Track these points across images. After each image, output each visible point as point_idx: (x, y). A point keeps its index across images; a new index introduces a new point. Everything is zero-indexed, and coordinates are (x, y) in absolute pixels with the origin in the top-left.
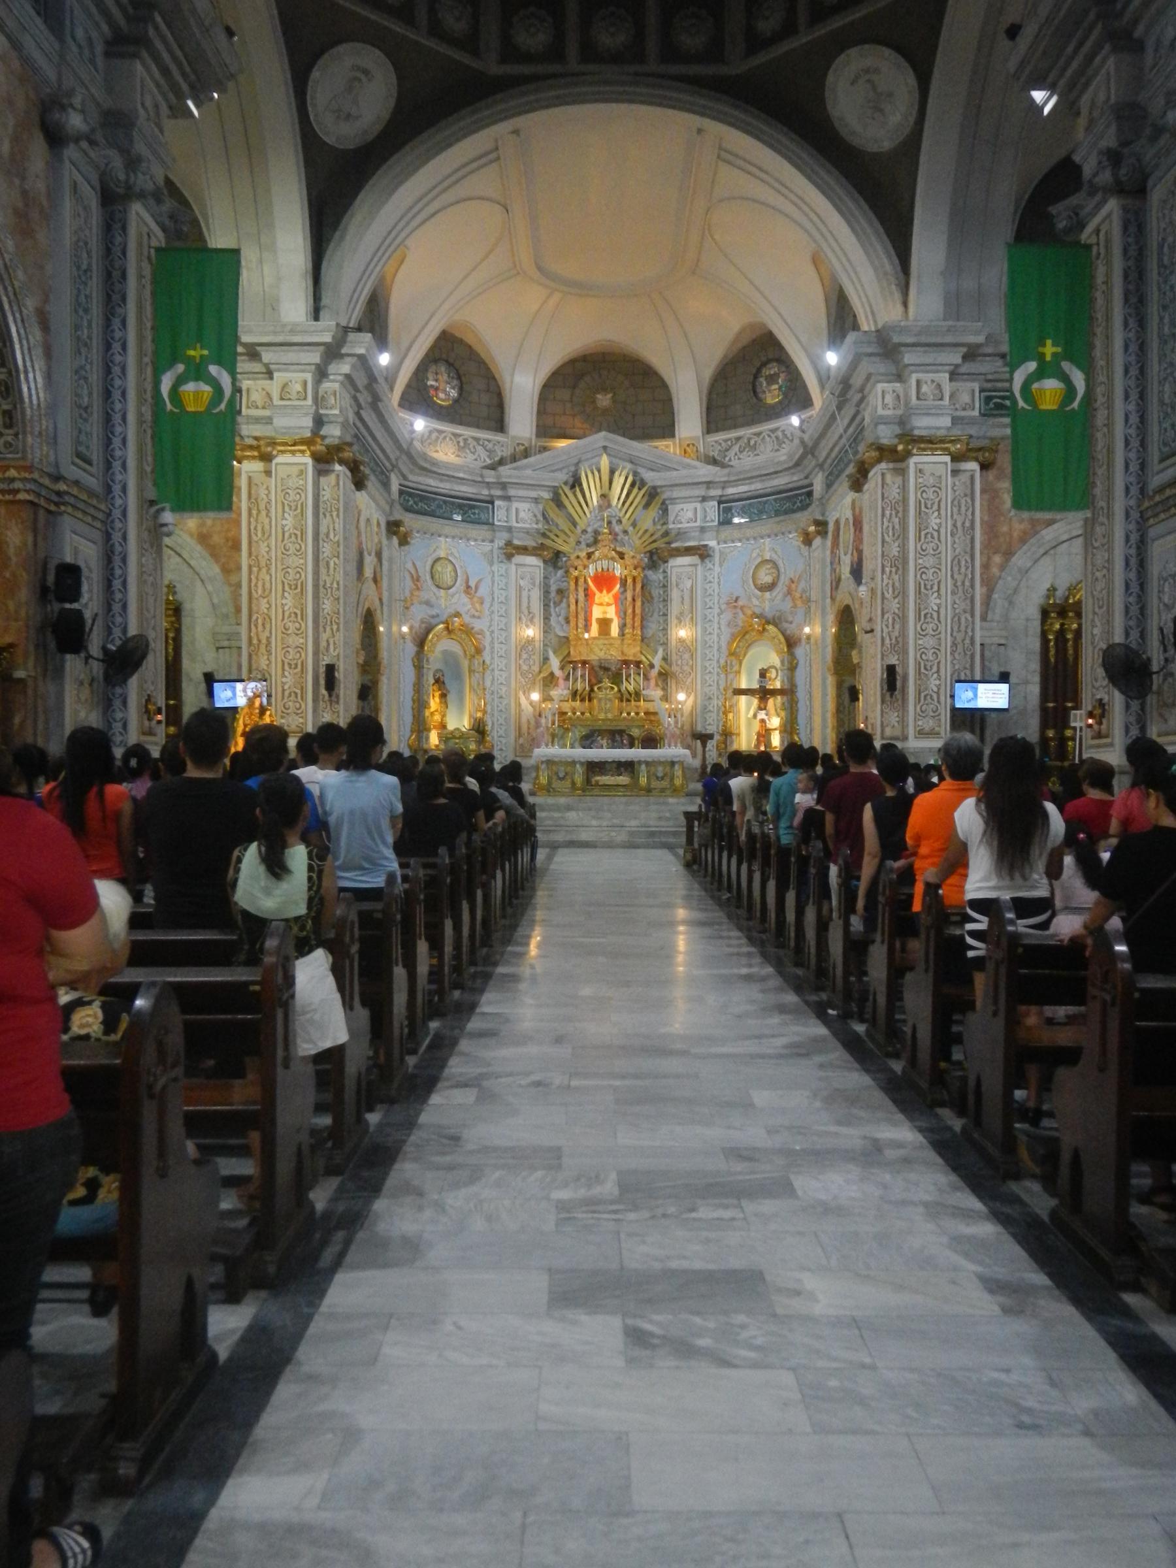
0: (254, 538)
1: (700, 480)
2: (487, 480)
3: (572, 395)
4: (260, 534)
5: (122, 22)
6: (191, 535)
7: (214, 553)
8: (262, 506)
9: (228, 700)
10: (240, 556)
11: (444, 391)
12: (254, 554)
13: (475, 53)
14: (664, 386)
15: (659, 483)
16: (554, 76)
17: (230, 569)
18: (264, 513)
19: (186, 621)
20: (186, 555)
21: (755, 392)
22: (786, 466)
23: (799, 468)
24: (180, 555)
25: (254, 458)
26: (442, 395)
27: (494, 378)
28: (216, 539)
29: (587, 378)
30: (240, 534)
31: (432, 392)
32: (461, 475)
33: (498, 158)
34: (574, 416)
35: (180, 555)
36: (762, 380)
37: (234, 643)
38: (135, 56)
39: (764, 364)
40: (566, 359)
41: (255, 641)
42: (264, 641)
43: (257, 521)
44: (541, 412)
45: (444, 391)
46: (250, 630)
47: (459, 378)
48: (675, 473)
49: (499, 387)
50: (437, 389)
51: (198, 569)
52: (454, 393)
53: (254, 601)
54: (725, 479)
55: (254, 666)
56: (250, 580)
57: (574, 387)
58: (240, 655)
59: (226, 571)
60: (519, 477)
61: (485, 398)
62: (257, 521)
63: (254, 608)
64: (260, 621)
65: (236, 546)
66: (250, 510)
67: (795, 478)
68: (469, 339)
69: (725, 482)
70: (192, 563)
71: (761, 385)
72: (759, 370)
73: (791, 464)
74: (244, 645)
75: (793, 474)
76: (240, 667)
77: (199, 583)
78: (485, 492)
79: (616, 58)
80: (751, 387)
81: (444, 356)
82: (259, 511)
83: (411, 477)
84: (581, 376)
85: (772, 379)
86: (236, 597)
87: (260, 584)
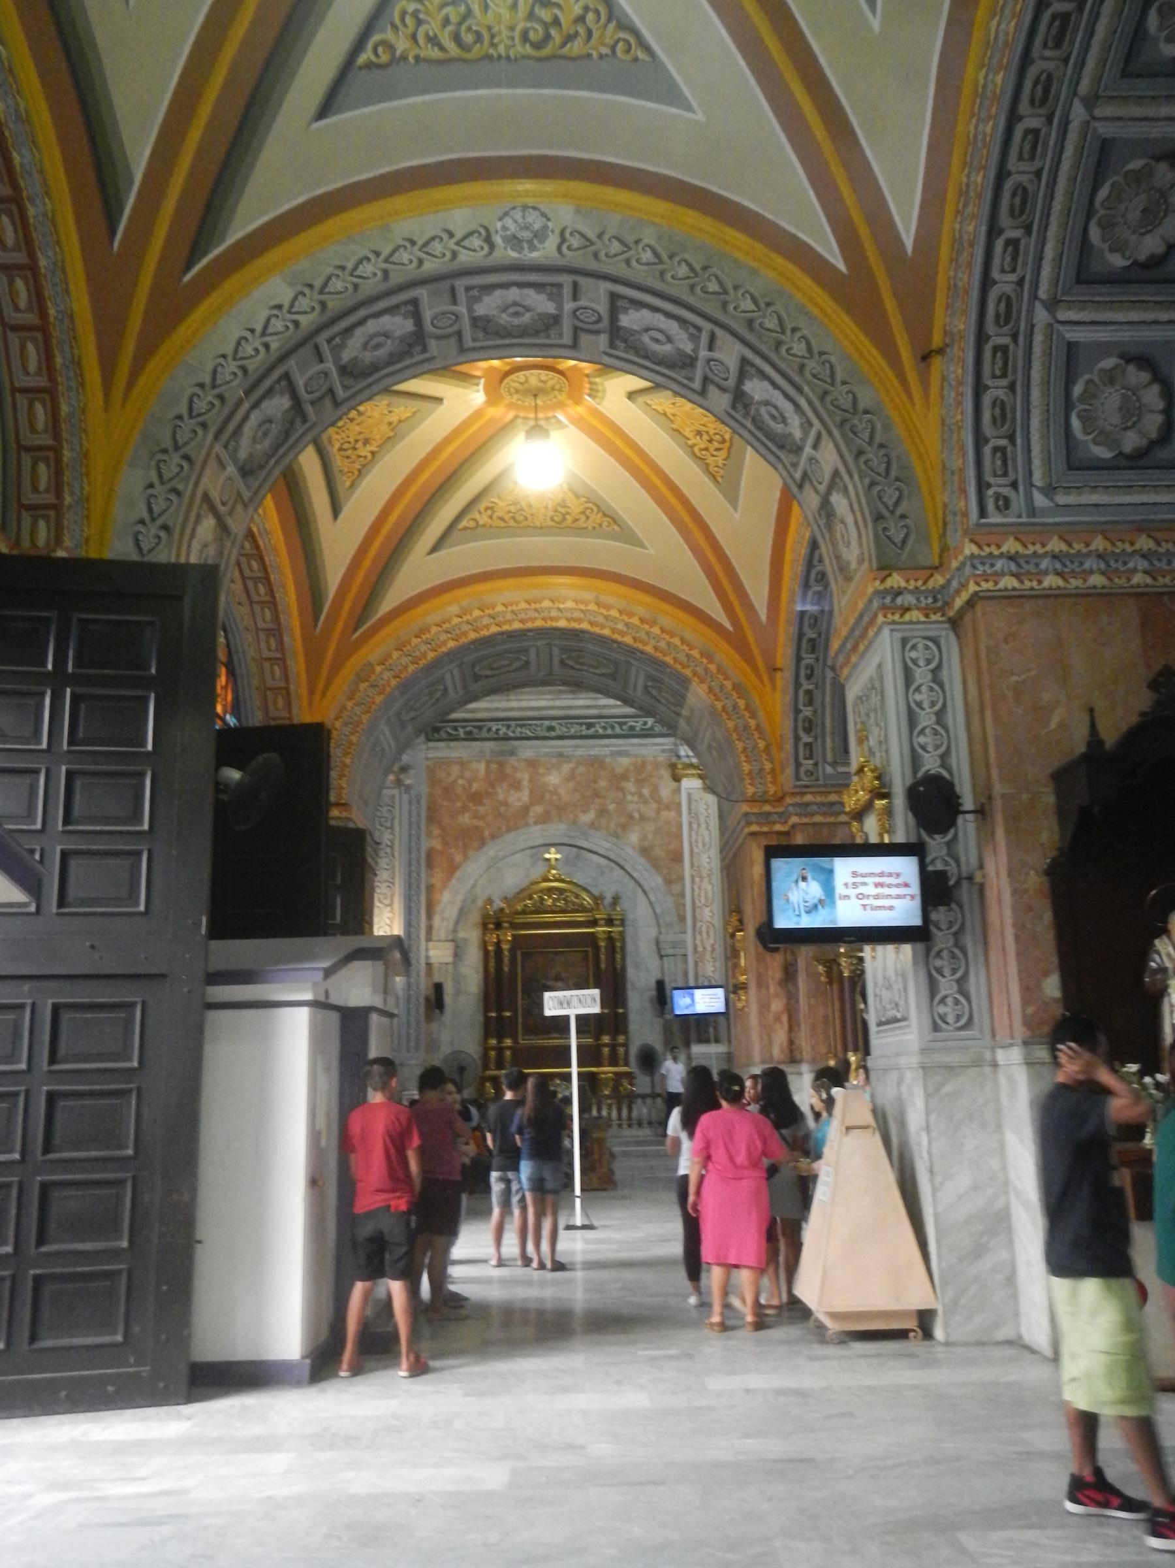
0: (696, 850)
4: (700, 846)
6: (634, 848)
7: (655, 864)
8: (702, 820)
9: (687, 1007)
10: (683, 867)
12: (696, 864)
17: (672, 880)
18: (703, 826)
20: (628, 867)
24: (622, 868)
25: (693, 775)
28: (657, 852)
30: (682, 846)
35: (622, 868)
37: (678, 951)
41: (700, 949)
42: (709, 949)
43: (697, 834)
46: (695, 939)
51: (642, 881)
53: (698, 910)
55: (700, 973)
56: (693, 890)
58: (686, 962)
59: (669, 882)
62: (697, 834)
63: (698, 915)
64: (704, 929)
65: (677, 858)
66: (690, 823)
70: (635, 875)
74: (690, 952)
76: (686, 974)
77: (641, 895)
82: (699, 825)
86: (680, 906)
87: (703, 894)
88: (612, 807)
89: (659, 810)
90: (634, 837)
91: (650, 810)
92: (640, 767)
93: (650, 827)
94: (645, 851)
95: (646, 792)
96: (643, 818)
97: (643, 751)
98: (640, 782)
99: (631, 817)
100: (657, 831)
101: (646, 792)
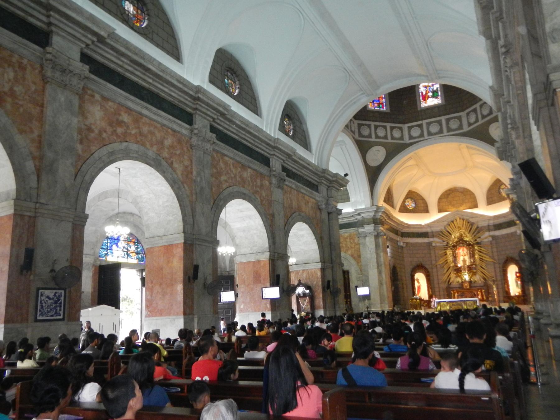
5: (328, 184)
7: (354, 258)
13: (403, 140)
14: (473, 194)
15: (474, 221)
16: (422, 141)
19: (350, 274)
27: (424, 199)
28: (355, 255)
29: (451, 195)
31: (408, 206)
38: (332, 189)
40: (445, 190)
44: (439, 206)
45: (411, 205)
47: (415, 201)
52: (414, 205)
59: (358, 263)
61: (422, 205)
68: (416, 191)
79: (436, 134)
84: (449, 194)
88: (344, 246)
89: (355, 246)
90: (349, 253)
91: (353, 246)
92: (350, 236)
93: (353, 250)
94: (352, 256)
95: (352, 241)
96: (351, 248)
97: (351, 231)
98: (351, 239)
99: (349, 248)
100: (355, 250)
101: (352, 241)
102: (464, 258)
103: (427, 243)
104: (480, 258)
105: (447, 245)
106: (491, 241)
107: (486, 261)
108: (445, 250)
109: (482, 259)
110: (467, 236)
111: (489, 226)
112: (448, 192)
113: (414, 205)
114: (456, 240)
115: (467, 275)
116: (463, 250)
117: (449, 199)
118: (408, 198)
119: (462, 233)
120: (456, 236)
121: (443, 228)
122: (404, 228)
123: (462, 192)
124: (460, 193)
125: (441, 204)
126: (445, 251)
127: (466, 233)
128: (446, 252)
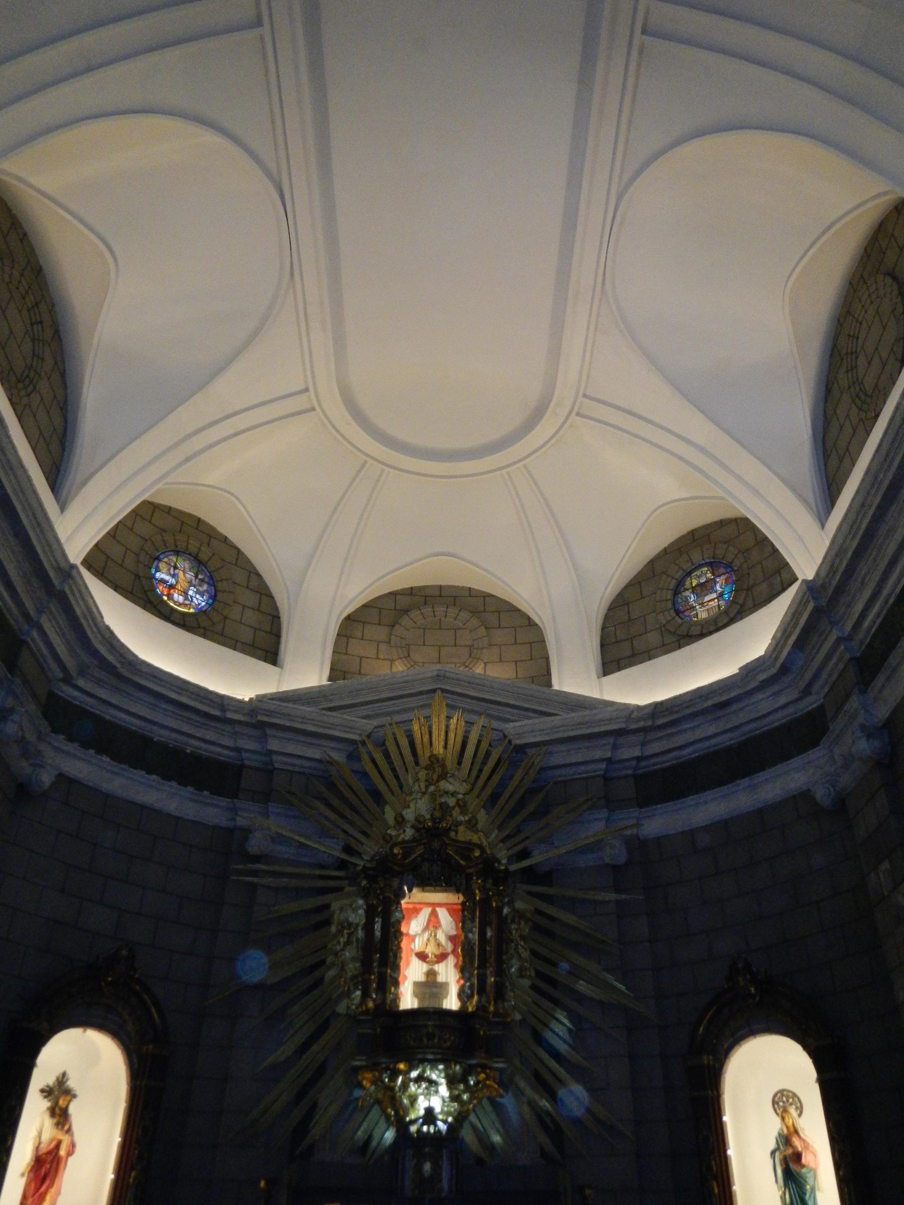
1: (603, 729)
2: (229, 715)
3: (391, 634)
11: (185, 593)
21: (678, 612)
22: (763, 677)
23: (787, 679)
26: (181, 599)
27: (270, 596)
29: (415, 614)
31: (160, 589)
32: (183, 699)
33: (259, 23)
34: (392, 661)
36: (687, 593)
39: (689, 574)
45: (185, 593)
47: (212, 581)
48: (556, 720)
49: (276, 609)
50: (171, 587)
54: (650, 723)
57: (393, 626)
60: (288, 716)
61: (251, 617)
67: (782, 700)
69: (644, 730)
71: (686, 600)
72: (680, 584)
73: (773, 671)
75: (776, 694)
78: (230, 743)
80: (670, 604)
81: (193, 549)
83: (81, 683)
84: (406, 611)
85: (704, 588)
102: (431, 974)
103: (215, 827)
104: (539, 974)
105: (342, 865)
106: (615, 868)
107: (581, 998)
108: (322, 891)
109: (553, 982)
110: (472, 825)
111: (606, 779)
112: (404, 601)
113: (200, 601)
114: (409, 833)
115: (444, 1090)
116: (433, 922)
117: (398, 630)
118: (177, 553)
119: (452, 802)
120: (409, 815)
121: (339, 757)
122: (82, 672)
123: (474, 613)
124: (464, 615)
125: (357, 648)
126: (318, 901)
127: (473, 803)
128: (327, 907)
